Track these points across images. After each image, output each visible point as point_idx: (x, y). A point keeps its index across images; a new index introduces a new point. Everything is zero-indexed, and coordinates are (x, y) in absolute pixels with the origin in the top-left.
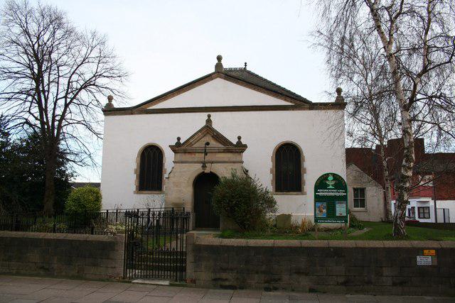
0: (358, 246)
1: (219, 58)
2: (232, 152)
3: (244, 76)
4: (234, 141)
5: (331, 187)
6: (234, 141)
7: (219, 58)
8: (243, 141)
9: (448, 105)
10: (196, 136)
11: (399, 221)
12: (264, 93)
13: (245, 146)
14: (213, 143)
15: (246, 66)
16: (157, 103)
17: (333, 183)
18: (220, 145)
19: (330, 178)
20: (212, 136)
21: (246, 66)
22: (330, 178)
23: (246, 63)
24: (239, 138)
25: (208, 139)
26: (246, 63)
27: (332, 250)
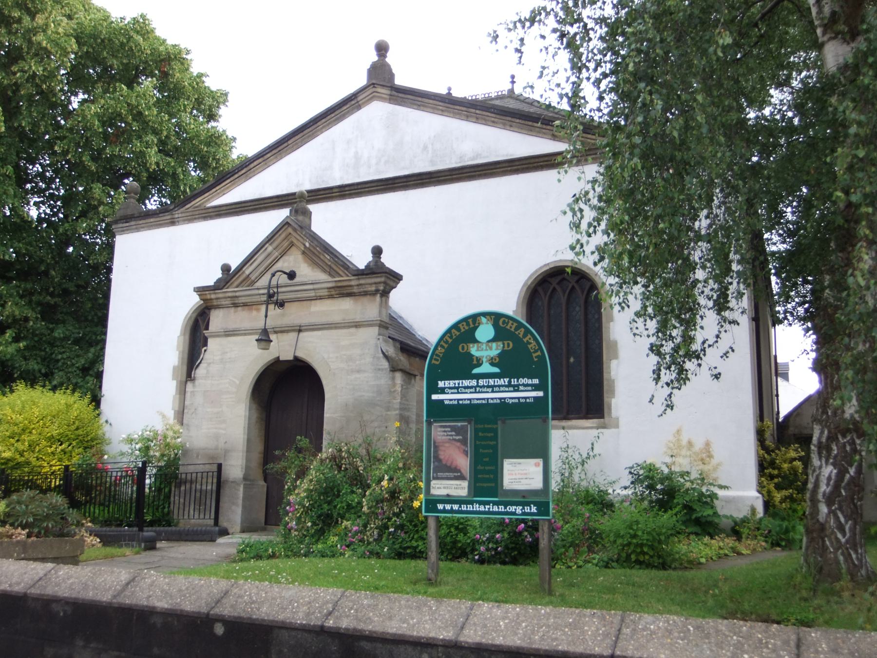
0: (789, 632)
1: (382, 49)
2: (350, 295)
3: (512, 104)
4: (361, 259)
5: (486, 368)
6: (361, 259)
7: (382, 49)
8: (387, 260)
9: (746, 3)
10: (260, 257)
11: (824, 509)
12: (494, 124)
13: (396, 278)
14: (306, 272)
15: (513, 82)
16: (235, 184)
17: (495, 351)
18: (322, 276)
19: (485, 332)
20: (304, 253)
21: (513, 82)
22: (485, 332)
23: (513, 77)
24: (377, 251)
25: (294, 261)
26: (513, 77)
27: (219, 629)
